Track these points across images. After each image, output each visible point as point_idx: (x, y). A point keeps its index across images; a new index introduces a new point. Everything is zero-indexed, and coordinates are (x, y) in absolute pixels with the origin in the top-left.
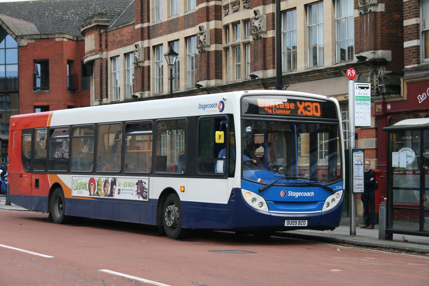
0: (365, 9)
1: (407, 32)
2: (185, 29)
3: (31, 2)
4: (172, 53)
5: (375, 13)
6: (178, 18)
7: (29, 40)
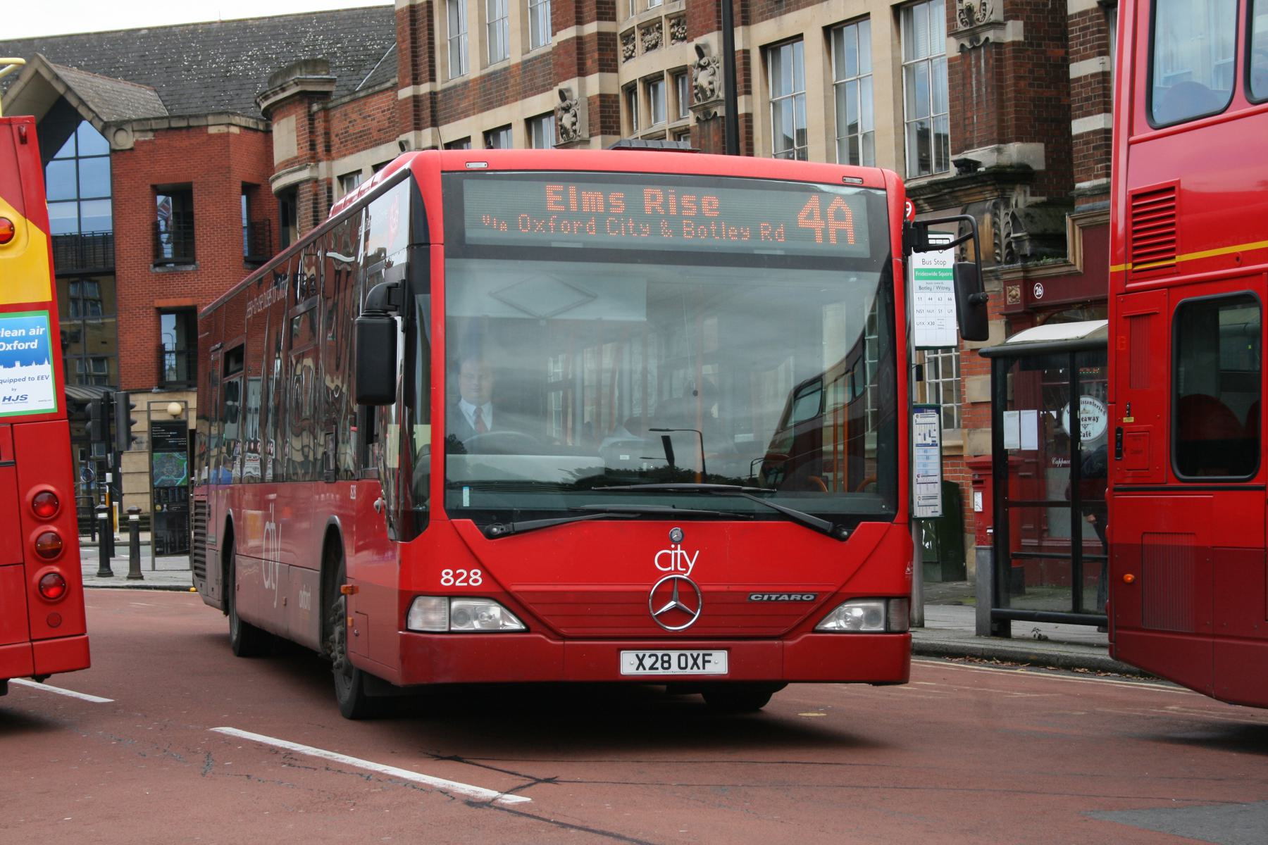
0: (973, 34)
1: (1079, 94)
2: (525, 97)
5: (999, 45)
6: (505, 69)
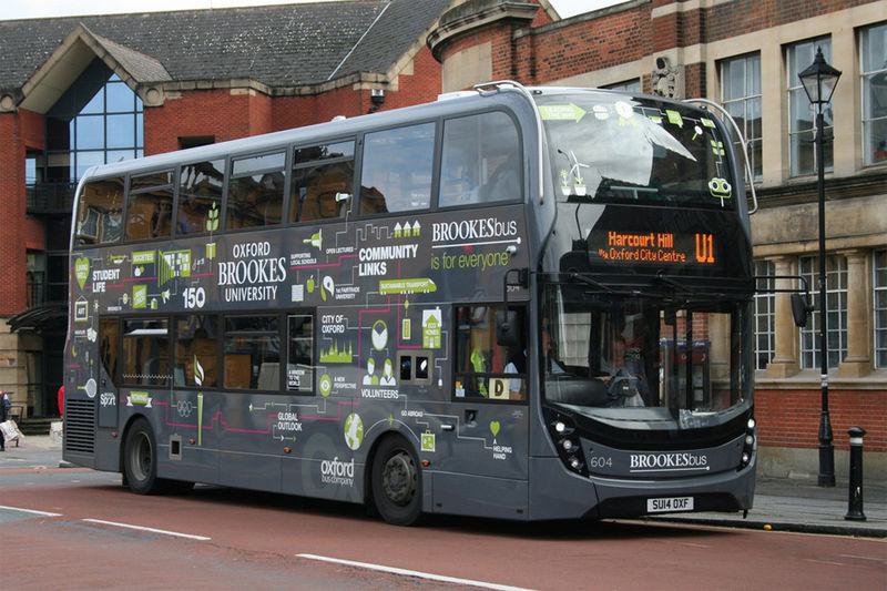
3: (145, 16)
7: (166, 94)
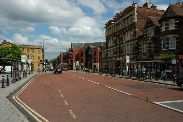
4: (110, 51)
